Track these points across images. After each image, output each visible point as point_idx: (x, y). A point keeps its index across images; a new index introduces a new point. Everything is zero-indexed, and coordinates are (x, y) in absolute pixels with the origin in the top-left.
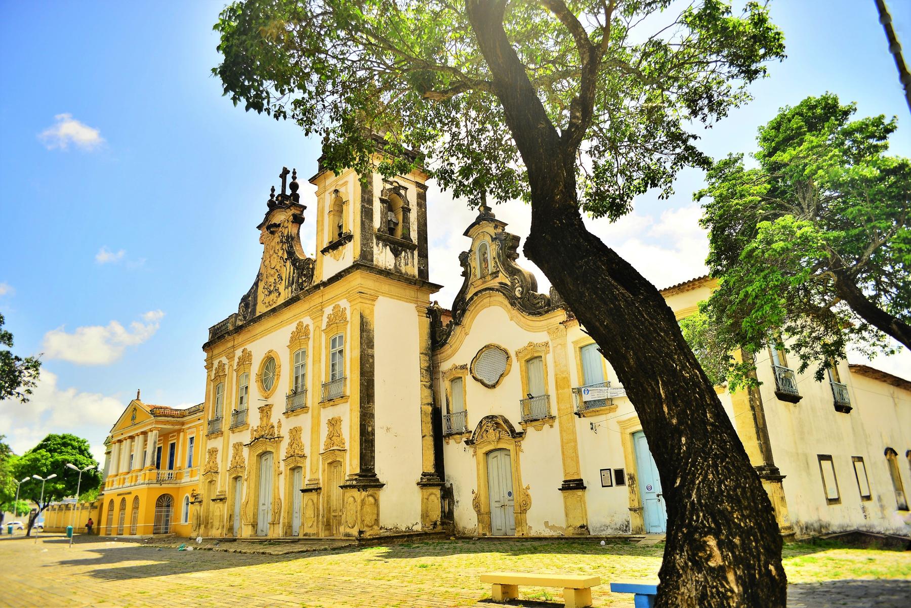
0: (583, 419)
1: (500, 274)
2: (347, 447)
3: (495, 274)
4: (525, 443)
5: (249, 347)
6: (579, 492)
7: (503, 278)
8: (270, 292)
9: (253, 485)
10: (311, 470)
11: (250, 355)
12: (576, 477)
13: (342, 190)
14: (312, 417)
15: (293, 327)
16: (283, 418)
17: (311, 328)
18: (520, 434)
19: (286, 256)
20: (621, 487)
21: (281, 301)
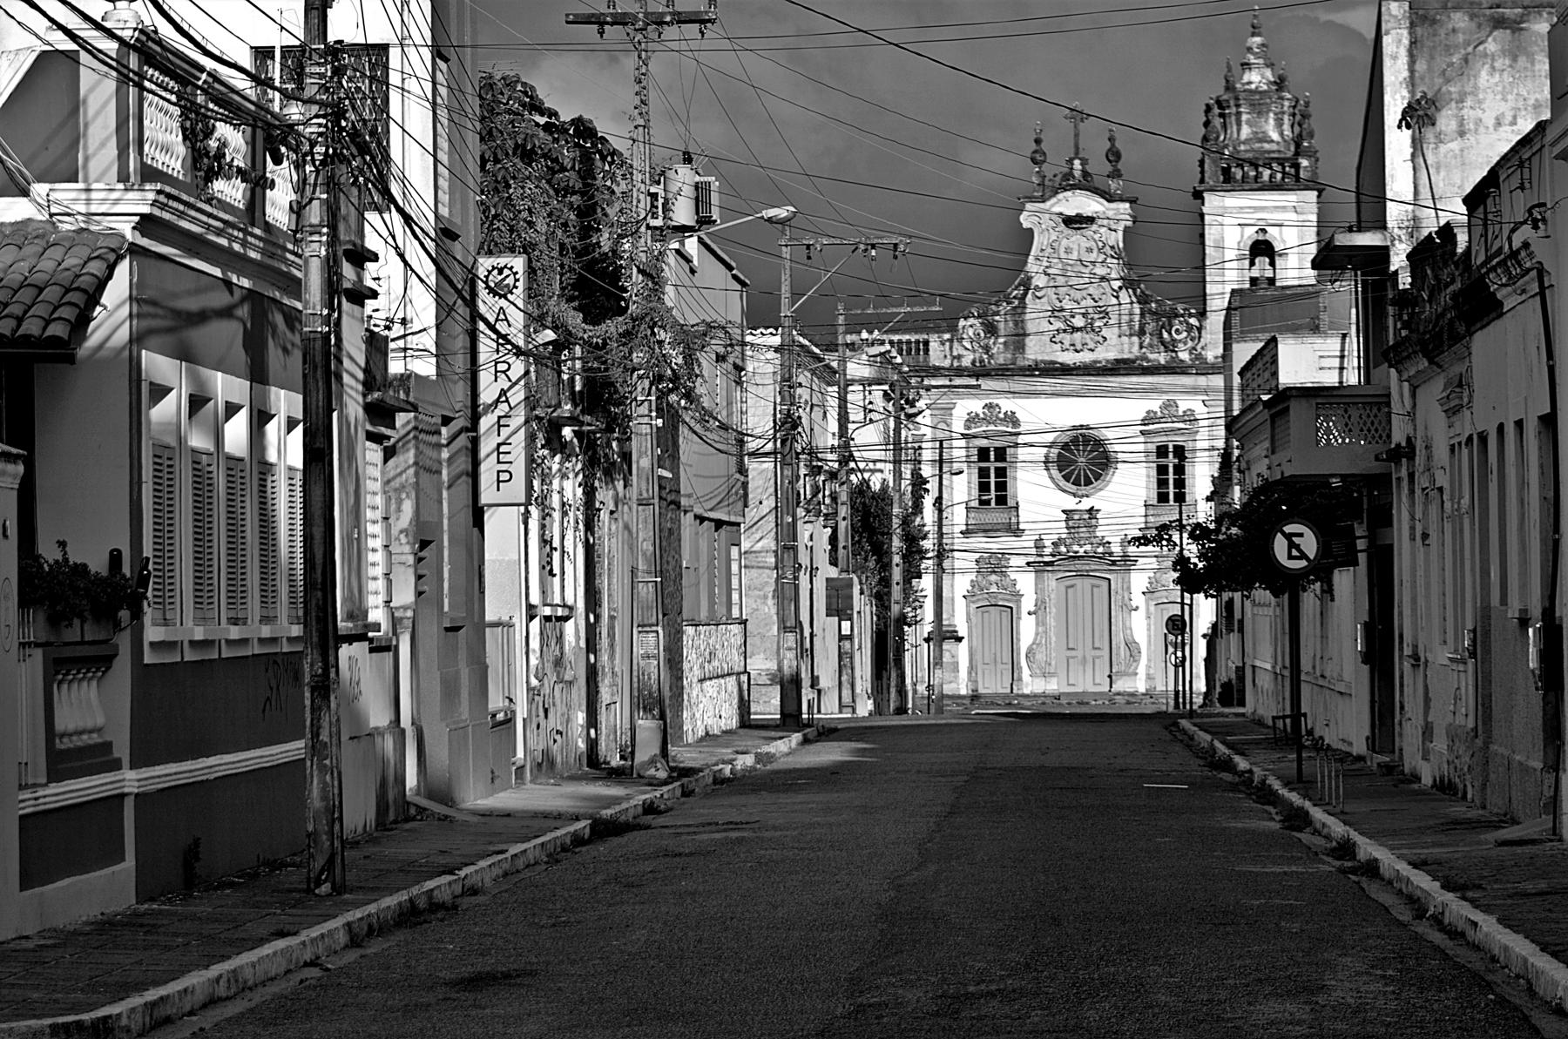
8: (1075, 329)
9: (1051, 621)
11: (1011, 419)
15: (1155, 405)
21: (1106, 354)
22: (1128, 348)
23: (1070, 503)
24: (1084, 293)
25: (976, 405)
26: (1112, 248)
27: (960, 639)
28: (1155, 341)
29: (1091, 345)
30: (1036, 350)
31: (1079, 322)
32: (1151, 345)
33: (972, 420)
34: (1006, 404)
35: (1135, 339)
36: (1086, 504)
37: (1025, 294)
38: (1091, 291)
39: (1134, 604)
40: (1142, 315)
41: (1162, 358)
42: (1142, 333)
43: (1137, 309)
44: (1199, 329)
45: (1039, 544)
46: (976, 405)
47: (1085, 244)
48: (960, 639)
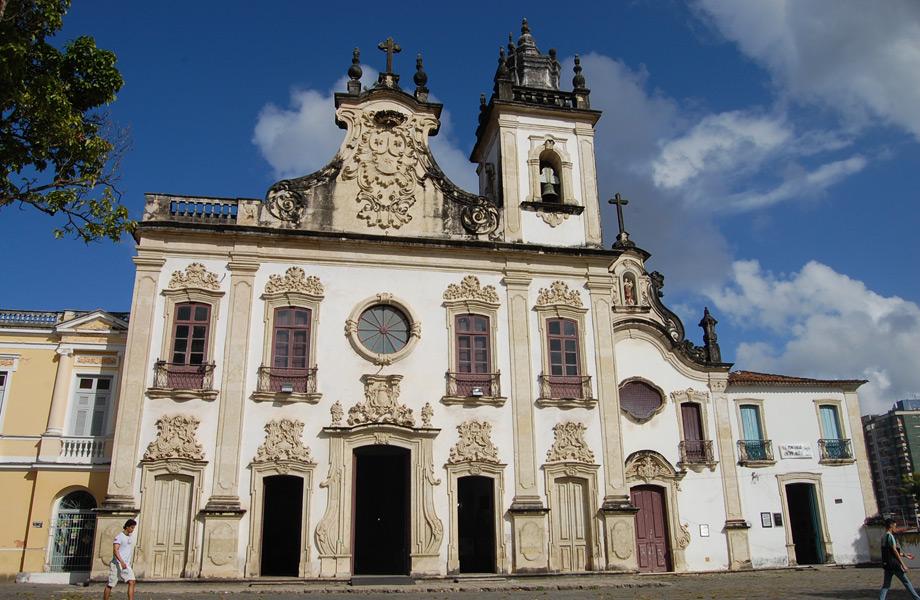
0: (744, 467)
1: (651, 311)
2: (598, 460)
3: (646, 309)
4: (682, 483)
5: (310, 270)
6: (744, 531)
7: (652, 315)
10: (519, 483)
11: (314, 282)
12: (739, 518)
13: (558, 147)
14: (516, 412)
15: (457, 278)
16: (438, 408)
17: (500, 290)
18: (684, 472)
19: (421, 173)
20: (779, 528)
22: (433, 229)
23: (371, 369)
24: (392, 178)
25: (280, 269)
26: (419, 143)
27: (241, 513)
28: (457, 223)
29: (397, 222)
30: (345, 220)
31: (385, 201)
32: (453, 227)
33: (275, 281)
34: (310, 270)
35: (440, 221)
36: (387, 371)
37: (336, 174)
38: (398, 176)
39: (436, 477)
40: (445, 202)
41: (464, 237)
42: (445, 215)
43: (440, 195)
44: (498, 217)
45: (334, 411)
46: (280, 269)
47: (393, 138)
48: (241, 513)
